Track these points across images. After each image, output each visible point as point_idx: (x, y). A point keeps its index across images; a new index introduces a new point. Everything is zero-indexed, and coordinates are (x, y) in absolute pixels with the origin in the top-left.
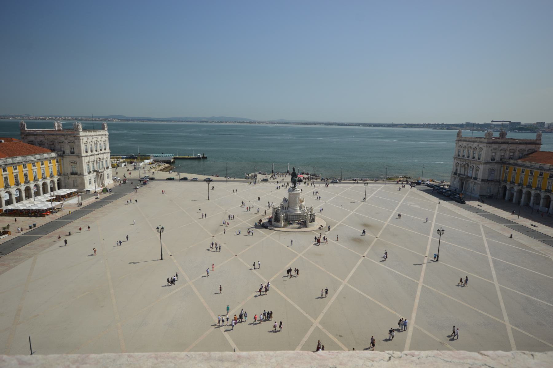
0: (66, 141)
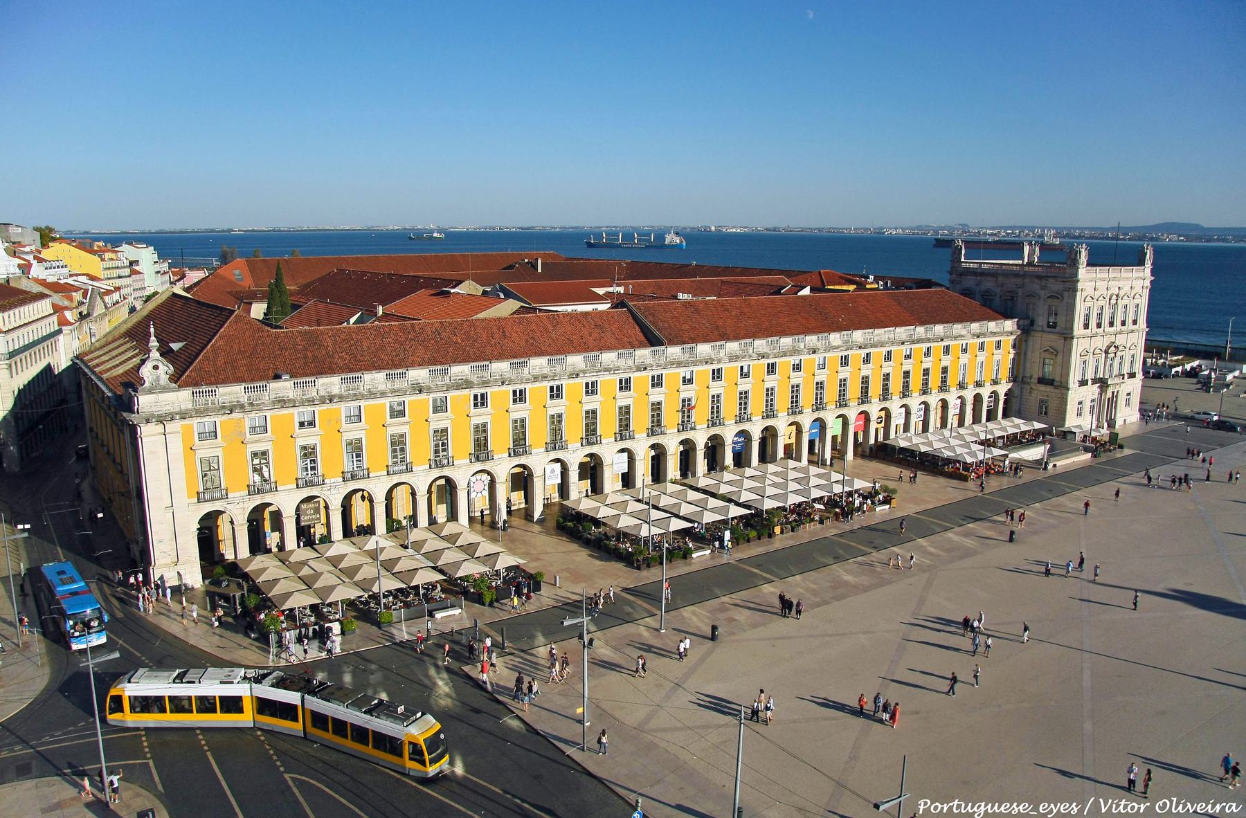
0: (1043, 293)
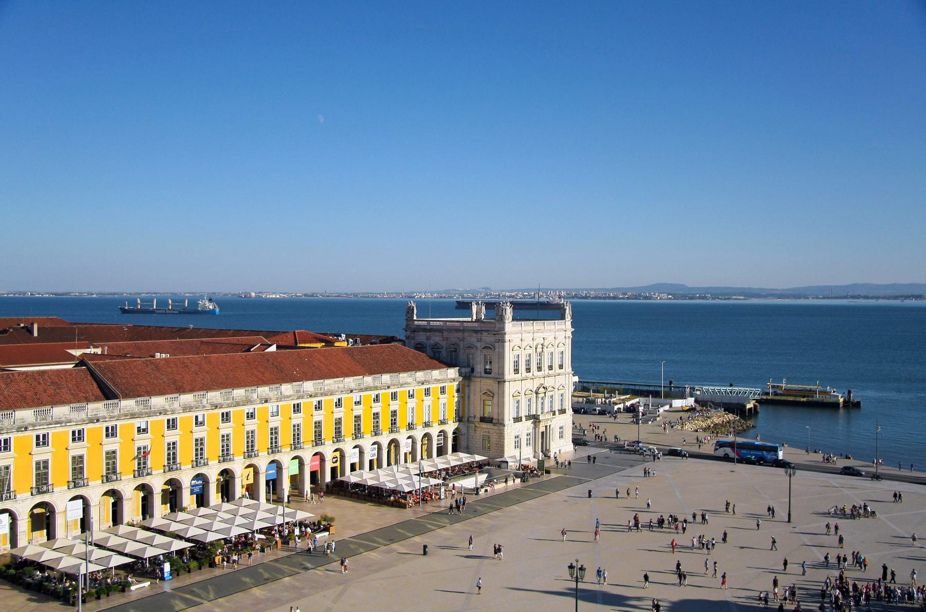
0: (478, 345)
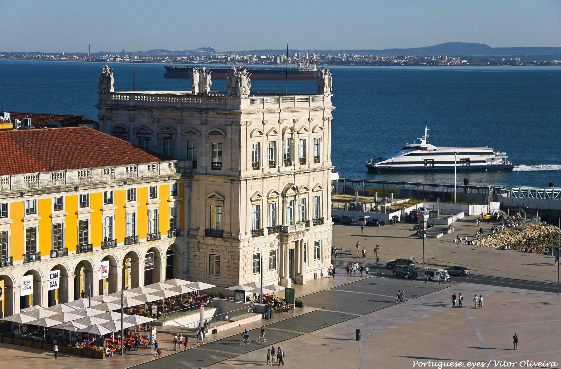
0: (203, 128)
